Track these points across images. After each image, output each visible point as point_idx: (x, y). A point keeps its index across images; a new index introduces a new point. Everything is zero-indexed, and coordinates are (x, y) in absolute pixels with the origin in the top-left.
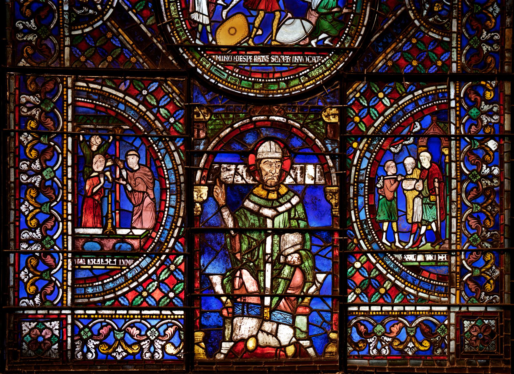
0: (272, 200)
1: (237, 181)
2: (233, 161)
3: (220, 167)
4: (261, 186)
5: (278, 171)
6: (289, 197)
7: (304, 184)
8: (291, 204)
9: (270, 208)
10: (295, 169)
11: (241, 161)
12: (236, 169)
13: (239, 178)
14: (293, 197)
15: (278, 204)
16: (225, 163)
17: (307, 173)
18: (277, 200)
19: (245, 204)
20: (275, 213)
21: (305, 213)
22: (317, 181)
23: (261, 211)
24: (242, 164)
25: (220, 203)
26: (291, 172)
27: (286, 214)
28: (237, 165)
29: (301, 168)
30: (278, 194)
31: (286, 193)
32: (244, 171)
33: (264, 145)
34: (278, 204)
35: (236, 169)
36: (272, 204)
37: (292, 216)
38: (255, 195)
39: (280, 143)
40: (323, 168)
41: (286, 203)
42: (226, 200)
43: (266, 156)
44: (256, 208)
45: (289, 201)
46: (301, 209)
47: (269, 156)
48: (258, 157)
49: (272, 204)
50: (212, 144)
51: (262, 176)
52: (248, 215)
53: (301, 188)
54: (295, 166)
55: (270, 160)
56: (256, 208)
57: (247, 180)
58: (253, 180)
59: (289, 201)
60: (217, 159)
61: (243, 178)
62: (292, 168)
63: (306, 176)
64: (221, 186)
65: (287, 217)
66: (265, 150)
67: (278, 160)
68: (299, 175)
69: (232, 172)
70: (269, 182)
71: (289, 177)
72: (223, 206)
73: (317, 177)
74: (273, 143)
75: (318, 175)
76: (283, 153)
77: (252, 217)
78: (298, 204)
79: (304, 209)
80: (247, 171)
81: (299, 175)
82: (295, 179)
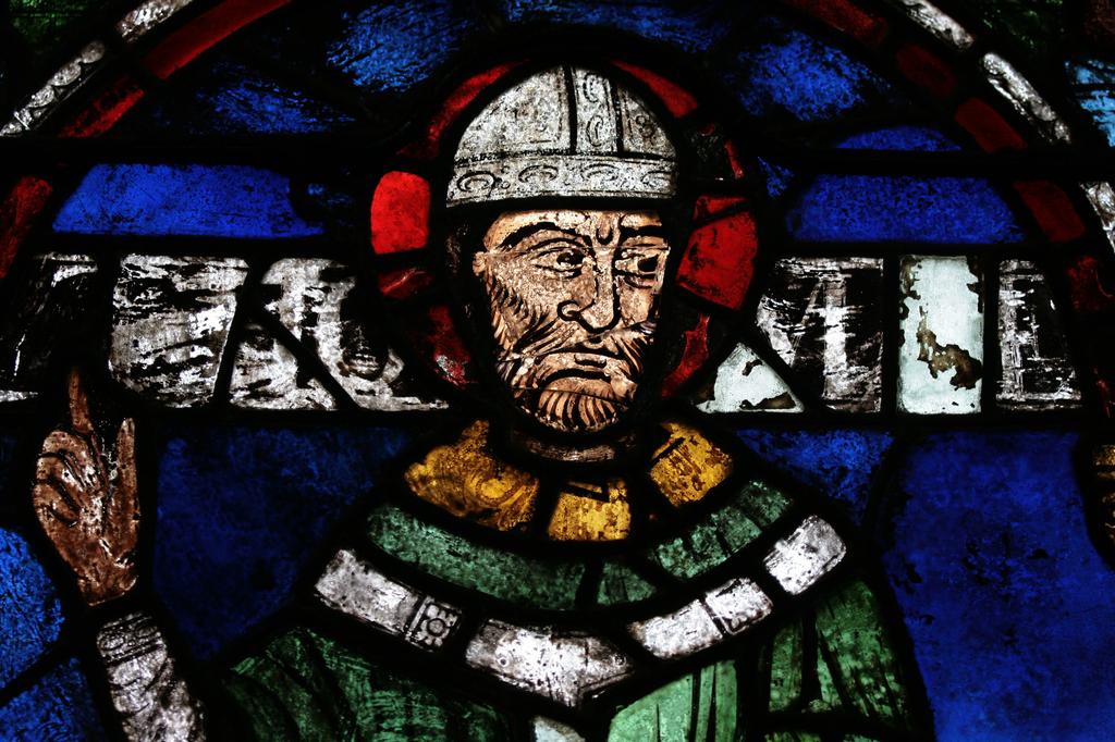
0: (591, 551)
1: (258, 389)
2: (226, 228)
3: (108, 273)
4: (477, 431)
5: (639, 304)
6: (745, 530)
7: (894, 419)
8: (770, 586)
9: (561, 625)
10: (799, 297)
11: (300, 229)
12: (255, 298)
13: (280, 370)
14: (784, 529)
15: (639, 591)
16: (150, 247)
17: (909, 327)
18: (635, 550)
19: (327, 586)
20: (616, 666)
21: (905, 665)
22: (1011, 391)
23: (476, 652)
24: (302, 252)
25: (90, 578)
26: (767, 319)
27: (721, 681)
28: (259, 258)
29: (859, 289)
30: (645, 499)
31: (718, 497)
32: (327, 309)
33: (510, 98)
34: (639, 591)
35: (255, 298)
36: (588, 591)
37: (779, 697)
38: (427, 513)
39: (656, 84)
40: (1055, 287)
41: (717, 579)
42: (143, 553)
43: (534, 187)
44: (436, 622)
45: (750, 565)
46: (869, 639)
47: (557, 187)
48: (454, 192)
49: (588, 591)
50: (44, 97)
51: (496, 346)
52: (356, 680)
53: (851, 451)
54: (800, 267)
55: (567, 219)
56: (436, 622)
57: (352, 385)
58: (399, 387)
59: (750, 565)
60: (81, 209)
61: (310, 368)
62: (773, 282)
63: (910, 350)
64: (110, 435)
65: (727, 705)
66: (519, 138)
67: (636, 221)
68: (835, 339)
69: (215, 318)
70: (555, 402)
71: (744, 355)
72: (114, 608)
73: (1010, 357)
74: (594, 89)
75: (1013, 340)
76: (685, 169)
77: (388, 699)
78: (827, 588)
79: (894, 634)
80: (347, 311)
81: (835, 339)
82: (805, 376)
